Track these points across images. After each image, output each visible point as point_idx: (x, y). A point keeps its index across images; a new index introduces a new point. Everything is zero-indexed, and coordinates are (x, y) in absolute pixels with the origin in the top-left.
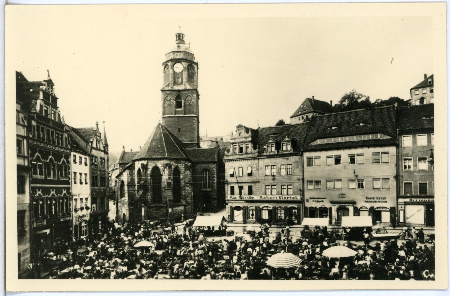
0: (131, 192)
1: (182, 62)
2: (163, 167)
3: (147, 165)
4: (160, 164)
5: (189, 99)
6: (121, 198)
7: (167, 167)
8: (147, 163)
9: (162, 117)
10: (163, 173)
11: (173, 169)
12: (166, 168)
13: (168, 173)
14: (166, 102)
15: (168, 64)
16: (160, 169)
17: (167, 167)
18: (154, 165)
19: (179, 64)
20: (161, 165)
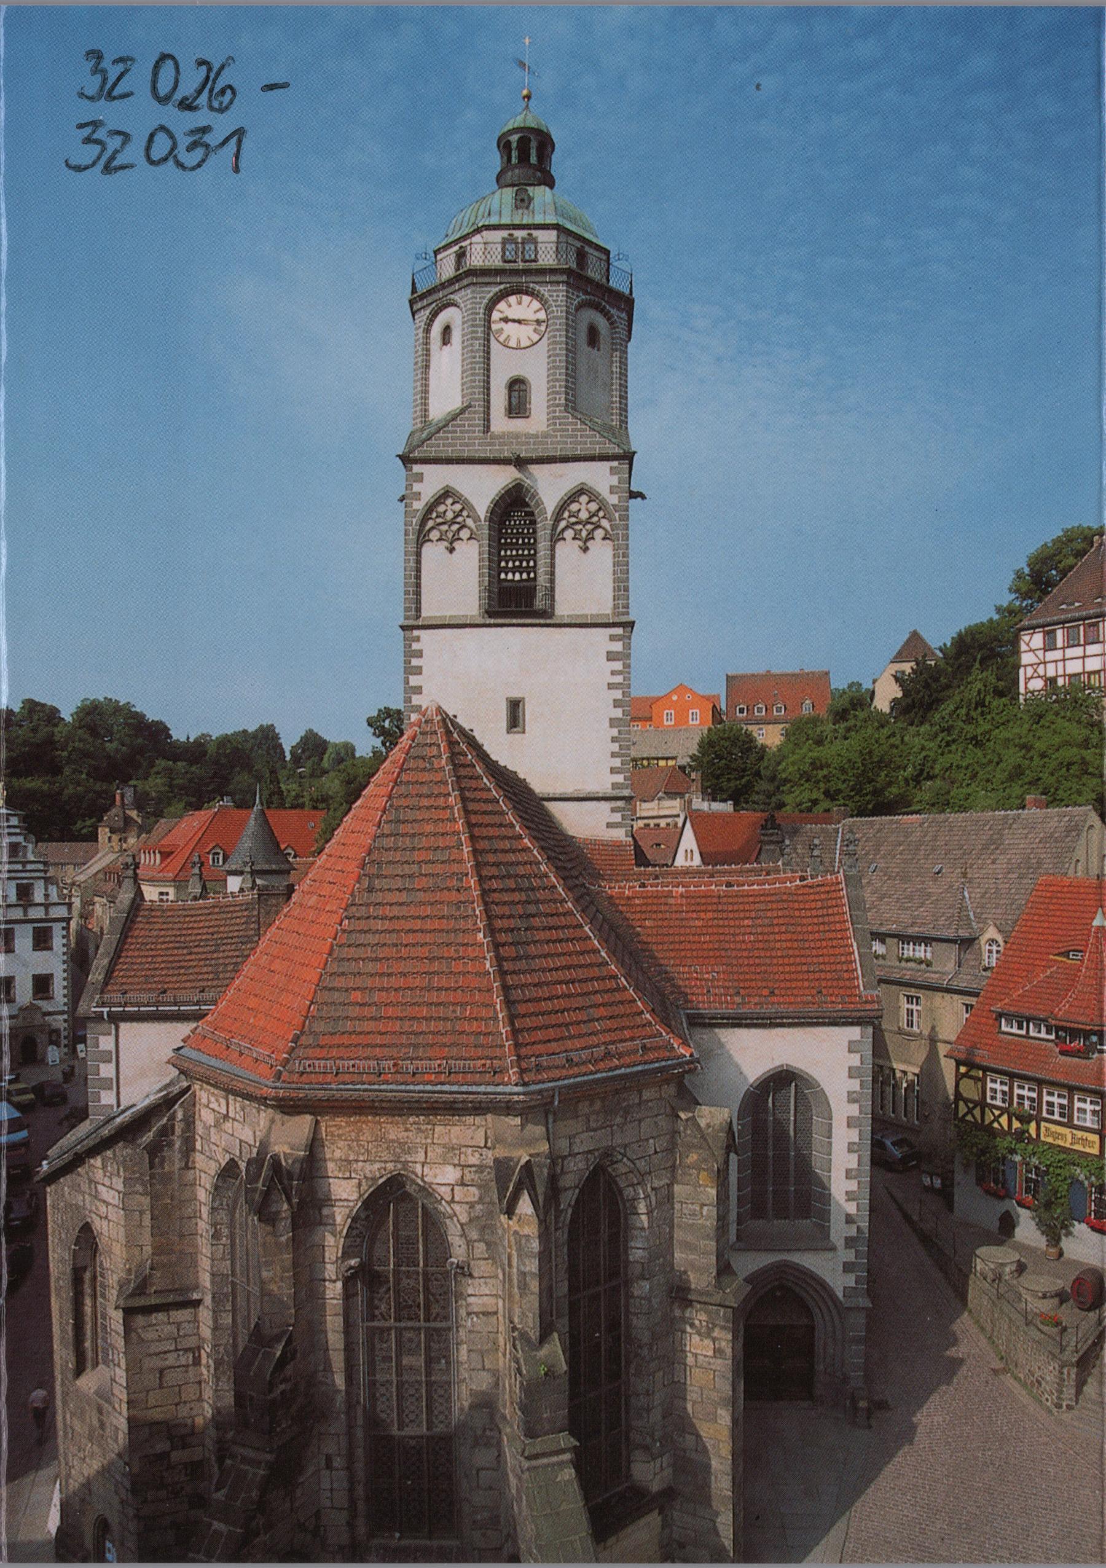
0: (161, 1372)
1: (544, 290)
2: (474, 1193)
3: (312, 1160)
4: (449, 1164)
5: (584, 515)
6: (79, 1371)
7: (525, 1206)
8: (314, 1145)
9: (403, 628)
10: (480, 1248)
11: (568, 1198)
12: (510, 1212)
13: (532, 1266)
14: (435, 535)
15: (456, 297)
16: (444, 1207)
17: (525, 1206)
18: (377, 1169)
19: (526, 299)
20: (450, 1174)
